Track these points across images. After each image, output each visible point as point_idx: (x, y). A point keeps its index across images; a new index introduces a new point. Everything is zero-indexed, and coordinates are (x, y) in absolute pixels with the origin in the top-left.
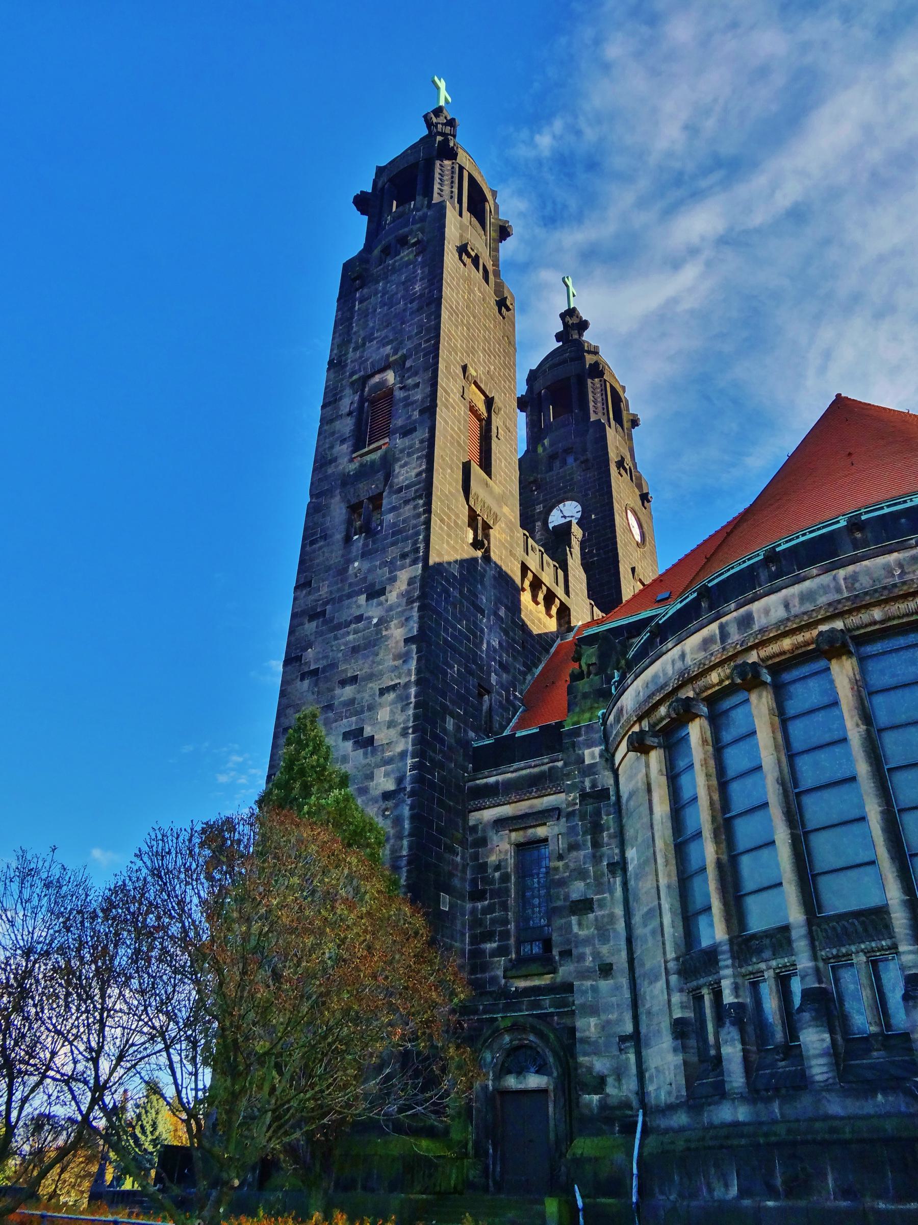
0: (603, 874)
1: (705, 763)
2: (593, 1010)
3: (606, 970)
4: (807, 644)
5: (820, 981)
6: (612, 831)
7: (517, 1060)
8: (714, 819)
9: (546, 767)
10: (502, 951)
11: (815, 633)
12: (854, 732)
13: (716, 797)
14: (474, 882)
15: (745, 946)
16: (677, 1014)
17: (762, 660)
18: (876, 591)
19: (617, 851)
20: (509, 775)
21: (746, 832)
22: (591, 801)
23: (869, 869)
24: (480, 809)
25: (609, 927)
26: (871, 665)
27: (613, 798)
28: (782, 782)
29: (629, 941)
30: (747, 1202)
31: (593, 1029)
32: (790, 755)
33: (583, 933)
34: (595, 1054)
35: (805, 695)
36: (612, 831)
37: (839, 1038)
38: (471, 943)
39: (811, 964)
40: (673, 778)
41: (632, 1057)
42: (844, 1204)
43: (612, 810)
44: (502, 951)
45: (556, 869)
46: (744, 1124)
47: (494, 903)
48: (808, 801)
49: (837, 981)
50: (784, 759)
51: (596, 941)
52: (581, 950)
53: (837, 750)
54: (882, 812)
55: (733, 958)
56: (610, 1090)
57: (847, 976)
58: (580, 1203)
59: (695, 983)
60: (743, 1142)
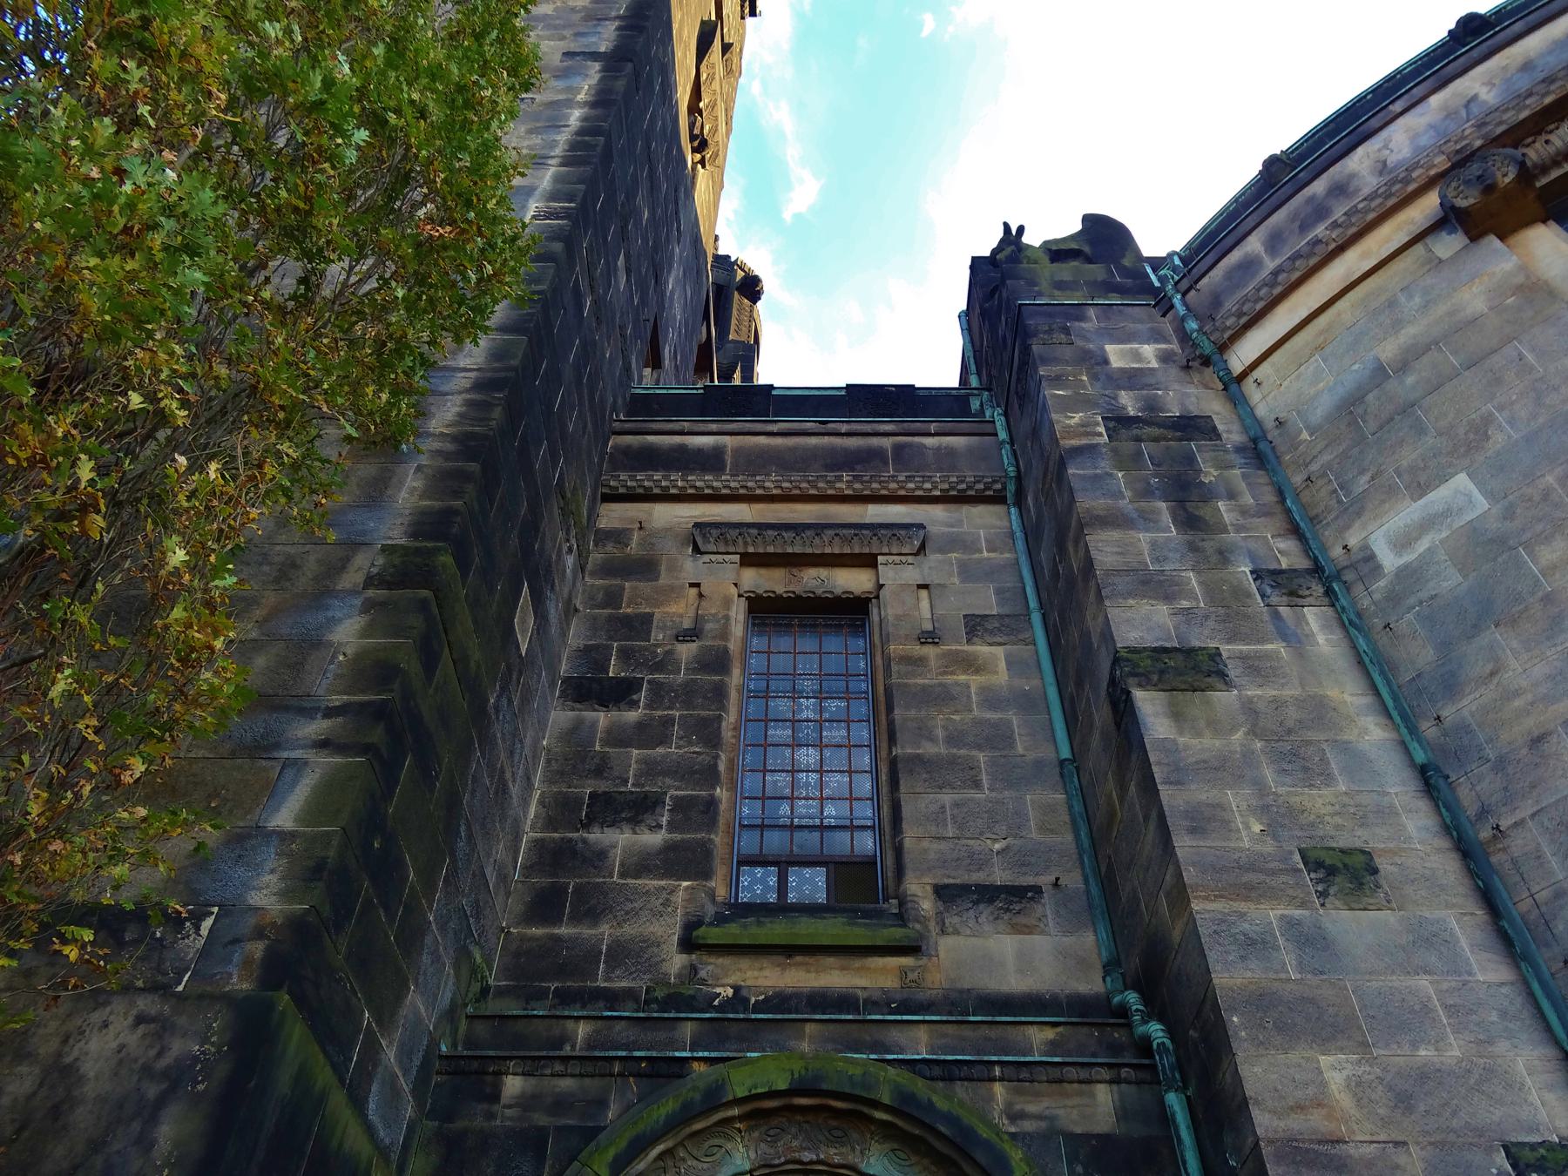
0: (1239, 593)
2: (1324, 1025)
3: (1346, 873)
14: (593, 656)
20: (762, 440)
24: (648, 497)
25: (1311, 735)
29: (1430, 780)
33: (1199, 745)
38: (550, 823)
45: (920, 661)
47: (668, 722)
51: (1269, 774)
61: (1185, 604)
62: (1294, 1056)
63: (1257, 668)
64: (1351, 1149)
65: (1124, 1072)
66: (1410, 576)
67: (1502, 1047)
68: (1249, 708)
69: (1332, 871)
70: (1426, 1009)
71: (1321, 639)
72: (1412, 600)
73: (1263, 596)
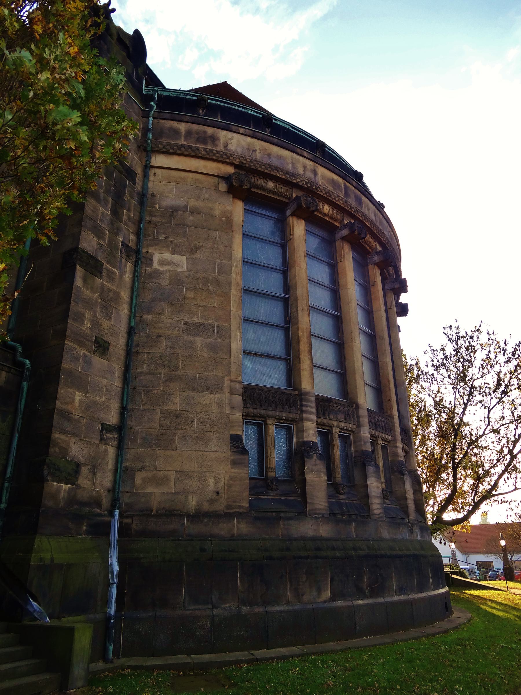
3: (102, 347)
29: (130, 331)
30: (340, 603)
31: (77, 404)
33: (87, 293)
34: (74, 434)
41: (112, 451)
46: (326, 539)
51: (98, 310)
56: (84, 481)
61: (102, 242)
62: (71, 390)
63: (110, 276)
64: (73, 416)
65: (12, 370)
66: (157, 274)
67: (112, 401)
68: (103, 286)
69: (100, 346)
70: (102, 388)
71: (127, 275)
72: (154, 280)
73: (121, 252)
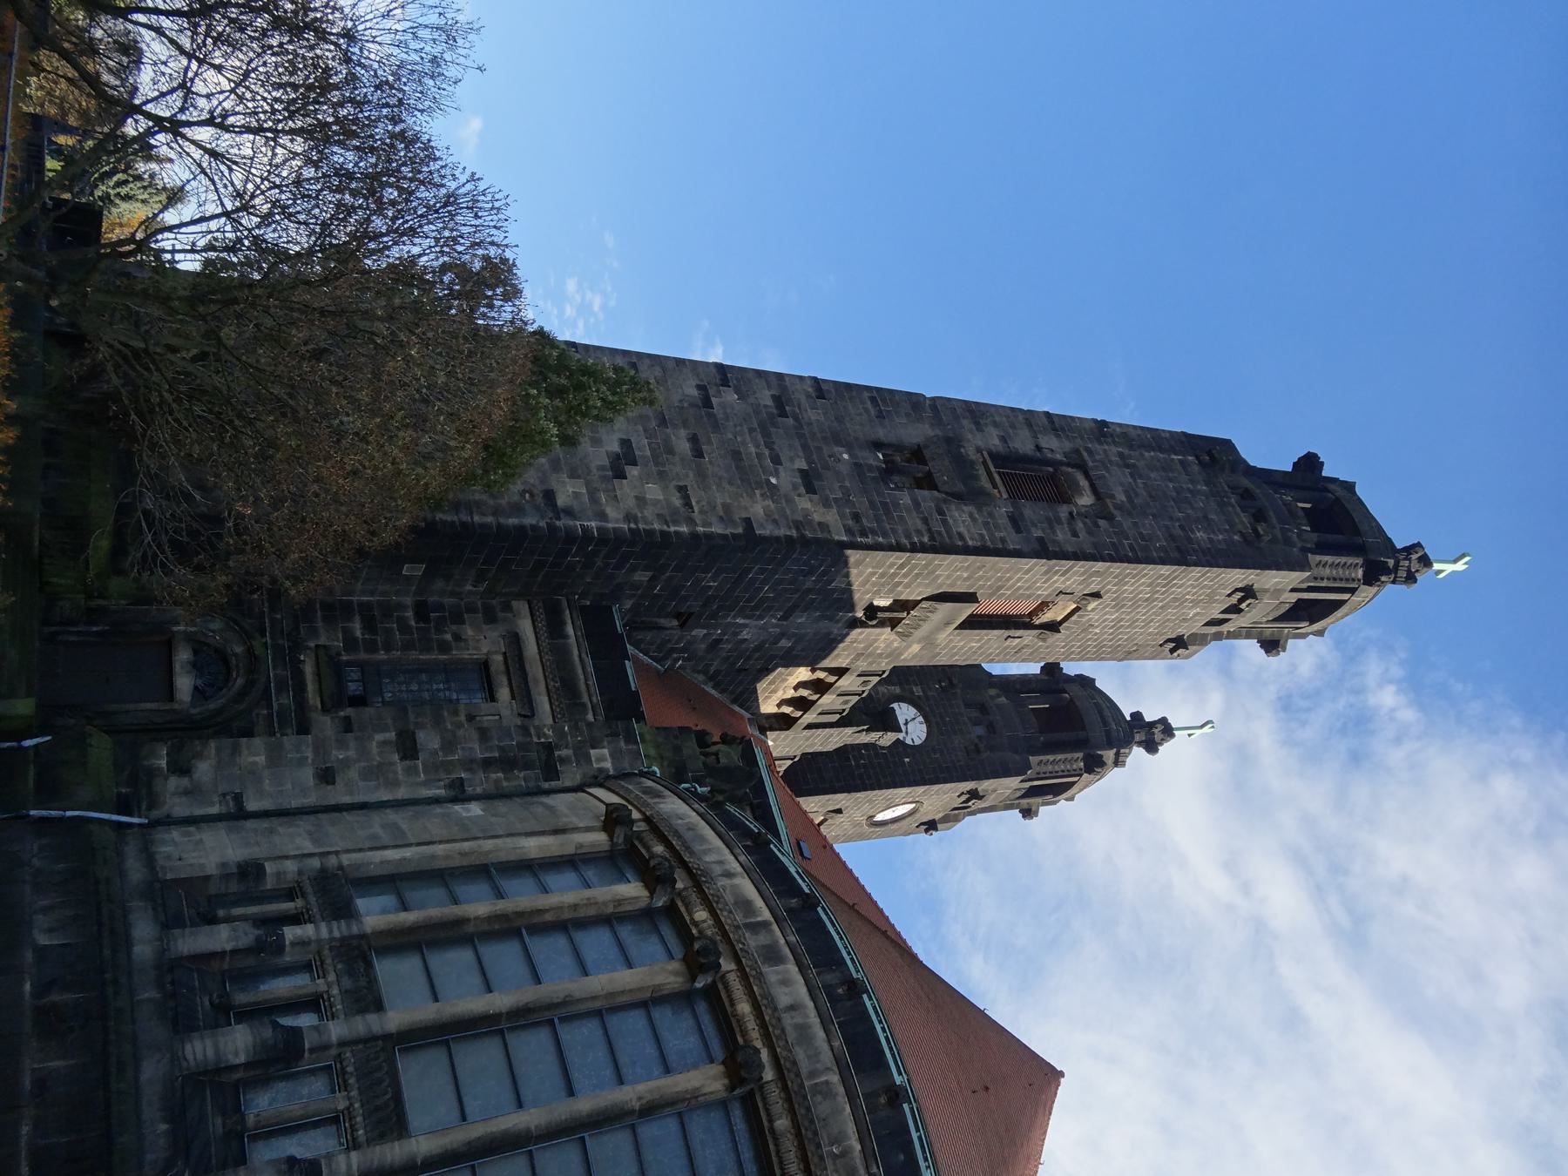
1: (590, 903)
2: (275, 759)
3: (326, 776)
4: (744, 1033)
5: (312, 1050)
6: (505, 784)
7: (211, 661)
8: (520, 914)
9: (585, 699)
10: (351, 643)
11: (758, 1044)
12: (630, 1094)
13: (548, 917)
14: (440, 607)
15: (358, 955)
16: (269, 868)
17: (723, 977)
18: (812, 1122)
19: (479, 790)
20: (576, 652)
21: (504, 956)
22: (543, 757)
23: (456, 1113)
24: (532, 615)
26: (716, 1116)
27: (546, 785)
28: (567, 1002)
29: (364, 806)
30: (29, 956)
31: (251, 759)
32: (603, 1011)
33: (374, 747)
35: (680, 1032)
36: (505, 784)
37: (240, 1075)
38: (361, 604)
39: (334, 1038)
40: (571, 862)
42: (27, 1082)
43: (531, 784)
44: (351, 643)
45: (456, 713)
46: (129, 954)
48: (542, 1036)
49: (312, 1072)
50: (597, 1005)
52: (352, 744)
53: (608, 1072)
54: (528, 1130)
55: (343, 939)
56: (174, 782)
57: (318, 1085)
58: (28, 743)
59: (309, 890)
60: (107, 952)
